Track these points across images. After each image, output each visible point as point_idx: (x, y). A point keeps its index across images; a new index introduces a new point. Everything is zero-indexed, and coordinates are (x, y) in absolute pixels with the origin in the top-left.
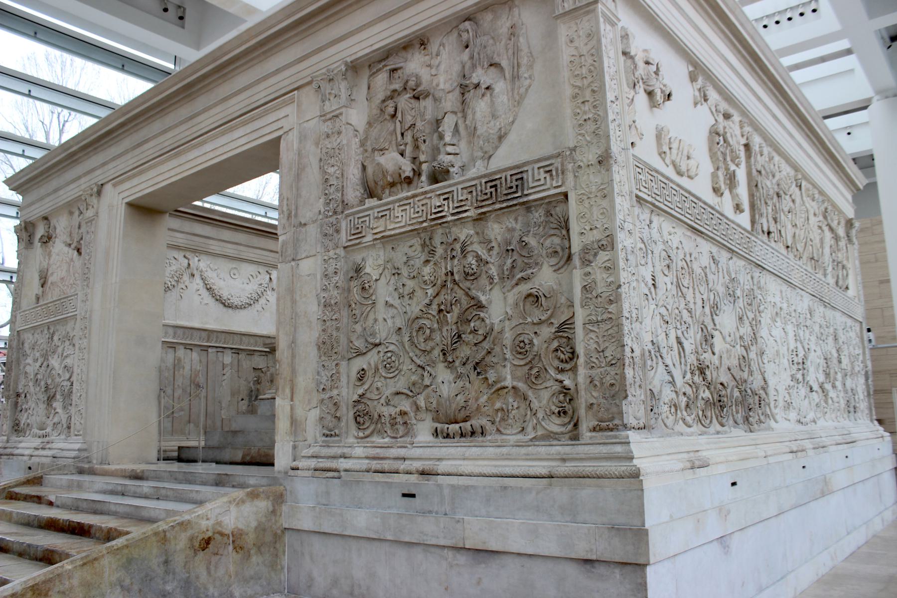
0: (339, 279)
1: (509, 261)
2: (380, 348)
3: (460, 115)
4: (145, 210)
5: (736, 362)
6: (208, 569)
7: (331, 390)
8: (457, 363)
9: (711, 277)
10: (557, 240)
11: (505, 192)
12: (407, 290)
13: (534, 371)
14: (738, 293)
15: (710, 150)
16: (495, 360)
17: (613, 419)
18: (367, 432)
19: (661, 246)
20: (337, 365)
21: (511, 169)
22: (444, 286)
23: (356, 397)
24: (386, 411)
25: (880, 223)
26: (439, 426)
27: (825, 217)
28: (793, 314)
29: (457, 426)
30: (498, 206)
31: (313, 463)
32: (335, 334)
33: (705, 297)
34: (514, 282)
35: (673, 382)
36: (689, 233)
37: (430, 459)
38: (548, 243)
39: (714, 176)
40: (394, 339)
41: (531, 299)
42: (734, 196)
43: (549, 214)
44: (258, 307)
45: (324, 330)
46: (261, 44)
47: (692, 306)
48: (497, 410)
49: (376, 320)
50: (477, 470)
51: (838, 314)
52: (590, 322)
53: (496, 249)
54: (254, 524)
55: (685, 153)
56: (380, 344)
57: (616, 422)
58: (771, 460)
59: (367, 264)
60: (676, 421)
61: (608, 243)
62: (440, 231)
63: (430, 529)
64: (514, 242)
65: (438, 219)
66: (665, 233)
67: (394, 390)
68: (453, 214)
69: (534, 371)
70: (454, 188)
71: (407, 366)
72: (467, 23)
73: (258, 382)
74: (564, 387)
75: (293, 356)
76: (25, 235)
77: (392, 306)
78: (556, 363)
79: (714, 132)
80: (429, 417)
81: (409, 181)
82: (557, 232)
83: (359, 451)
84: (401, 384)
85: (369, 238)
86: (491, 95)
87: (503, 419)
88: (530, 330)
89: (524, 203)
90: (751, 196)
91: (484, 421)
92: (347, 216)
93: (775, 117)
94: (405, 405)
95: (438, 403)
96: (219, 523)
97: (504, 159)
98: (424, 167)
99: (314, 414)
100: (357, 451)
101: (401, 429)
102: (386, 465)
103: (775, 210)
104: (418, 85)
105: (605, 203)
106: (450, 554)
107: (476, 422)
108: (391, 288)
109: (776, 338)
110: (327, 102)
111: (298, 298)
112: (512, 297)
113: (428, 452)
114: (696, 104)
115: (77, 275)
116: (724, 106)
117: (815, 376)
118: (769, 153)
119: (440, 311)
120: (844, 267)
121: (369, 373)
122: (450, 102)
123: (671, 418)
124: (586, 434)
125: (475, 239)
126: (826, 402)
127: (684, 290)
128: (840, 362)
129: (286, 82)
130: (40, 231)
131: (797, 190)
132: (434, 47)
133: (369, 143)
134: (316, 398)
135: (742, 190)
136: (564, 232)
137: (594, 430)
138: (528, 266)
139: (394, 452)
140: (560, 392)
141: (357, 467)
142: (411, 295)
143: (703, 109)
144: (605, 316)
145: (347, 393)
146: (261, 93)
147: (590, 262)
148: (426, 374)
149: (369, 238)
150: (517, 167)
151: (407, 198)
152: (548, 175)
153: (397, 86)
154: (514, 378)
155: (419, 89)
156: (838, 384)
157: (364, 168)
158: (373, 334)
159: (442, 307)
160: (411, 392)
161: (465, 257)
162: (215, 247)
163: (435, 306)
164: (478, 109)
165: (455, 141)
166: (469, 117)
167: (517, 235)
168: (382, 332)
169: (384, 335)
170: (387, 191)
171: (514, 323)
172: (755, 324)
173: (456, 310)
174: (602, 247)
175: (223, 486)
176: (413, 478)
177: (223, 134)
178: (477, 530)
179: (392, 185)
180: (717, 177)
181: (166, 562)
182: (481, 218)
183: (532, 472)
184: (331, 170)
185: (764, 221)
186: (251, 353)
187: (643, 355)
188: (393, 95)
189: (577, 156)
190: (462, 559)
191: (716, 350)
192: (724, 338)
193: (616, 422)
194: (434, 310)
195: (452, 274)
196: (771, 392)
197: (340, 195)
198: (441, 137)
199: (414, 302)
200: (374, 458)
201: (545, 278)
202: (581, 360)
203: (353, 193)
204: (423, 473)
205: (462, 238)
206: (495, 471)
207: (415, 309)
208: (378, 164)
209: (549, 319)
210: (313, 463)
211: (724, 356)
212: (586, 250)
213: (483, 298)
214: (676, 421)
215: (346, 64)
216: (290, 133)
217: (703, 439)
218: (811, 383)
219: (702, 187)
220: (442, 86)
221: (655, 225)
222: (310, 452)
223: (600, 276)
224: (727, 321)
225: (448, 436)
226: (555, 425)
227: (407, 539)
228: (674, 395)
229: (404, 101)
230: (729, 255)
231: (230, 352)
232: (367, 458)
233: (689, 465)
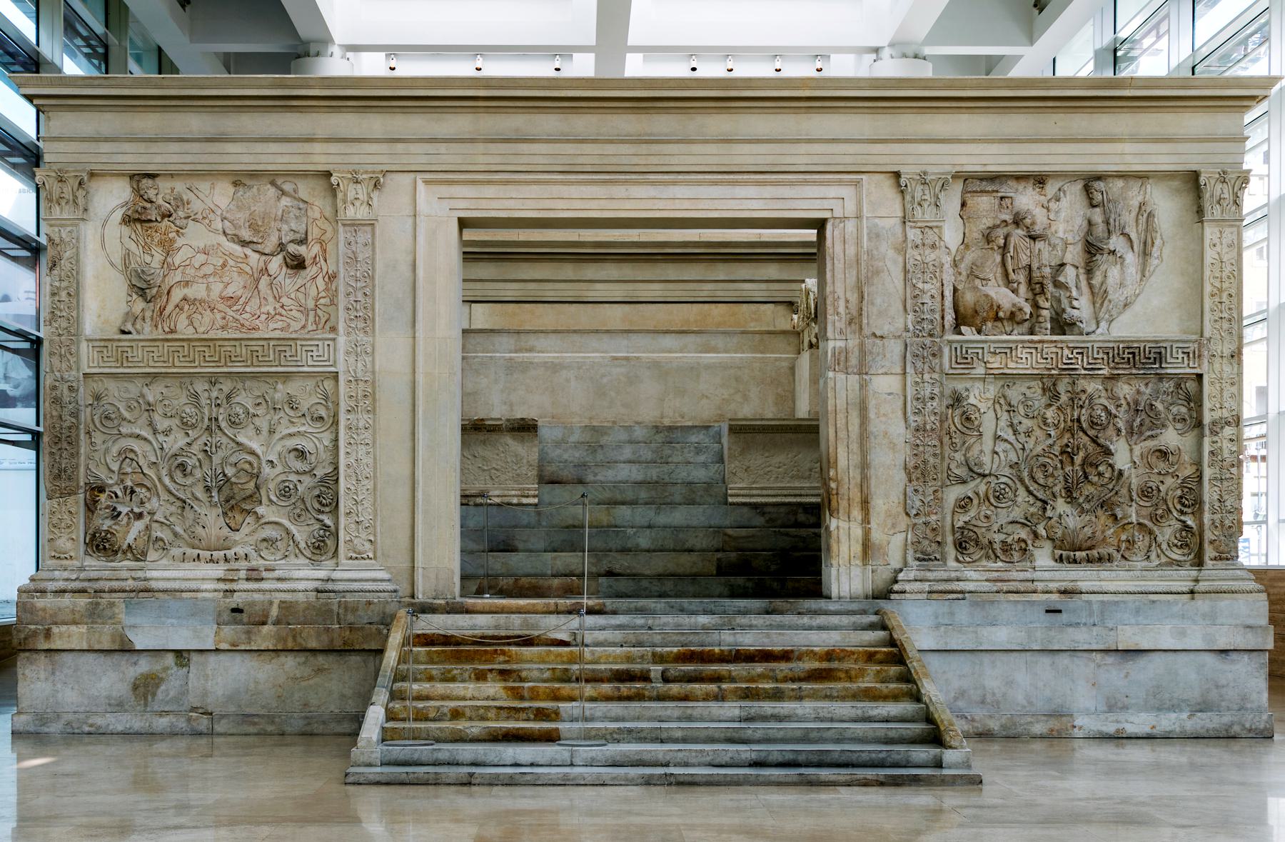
2: (988, 479)
3: (1081, 271)
7: (928, 515)
8: (1081, 500)
10: (1184, 410)
11: (1141, 359)
20: (935, 491)
22: (1070, 430)
24: (998, 538)
29: (1084, 554)
30: (1134, 371)
31: (926, 587)
32: (932, 460)
38: (1175, 409)
40: (1007, 471)
43: (1178, 386)
52: (1215, 479)
53: (1125, 406)
56: (990, 475)
61: (1237, 421)
63: (1082, 638)
65: (1069, 371)
67: (1010, 519)
74: (1187, 526)
75: (865, 478)
78: (1179, 507)
80: (1048, 546)
83: (974, 575)
84: (1017, 514)
85: (980, 370)
86: (1122, 264)
87: (1128, 548)
88: (1156, 478)
91: (1111, 550)
94: (1024, 534)
95: (1064, 534)
98: (1046, 313)
100: (975, 576)
101: (1016, 556)
104: (1033, 223)
105: (1234, 389)
106: (1098, 656)
107: (1104, 551)
108: (1002, 423)
111: (872, 415)
112: (1137, 450)
113: (1057, 575)
115: (284, 300)
119: (1062, 453)
121: (976, 502)
122: (1074, 254)
124: (1209, 563)
125: (1103, 394)
129: (848, 160)
132: (1051, 188)
133: (963, 266)
134: (904, 522)
137: (1215, 559)
139: (1015, 575)
140: (1181, 530)
142: (1028, 434)
145: (947, 518)
146: (800, 156)
149: (980, 370)
150: (1157, 342)
151: (1032, 342)
153: (1008, 218)
157: (955, 290)
158: (980, 465)
160: (1027, 522)
164: (1109, 274)
166: (1097, 281)
170: (989, 324)
171: (1141, 471)
173: (1081, 454)
176: (1055, 597)
177: (715, 183)
178: (1128, 637)
182: (1113, 378)
183: (1174, 590)
184: (920, 285)
189: (1212, 346)
190: (1110, 659)
194: (1057, 450)
195: (1079, 420)
197: (938, 316)
199: (1032, 441)
201: (1171, 437)
202: (1207, 507)
203: (950, 317)
204: (1064, 592)
207: (1037, 444)
208: (987, 296)
210: (926, 587)
212: (1214, 423)
213: (1111, 447)
216: (850, 226)
222: (912, 576)
223: (1226, 445)
225: (1075, 561)
226: (1176, 555)
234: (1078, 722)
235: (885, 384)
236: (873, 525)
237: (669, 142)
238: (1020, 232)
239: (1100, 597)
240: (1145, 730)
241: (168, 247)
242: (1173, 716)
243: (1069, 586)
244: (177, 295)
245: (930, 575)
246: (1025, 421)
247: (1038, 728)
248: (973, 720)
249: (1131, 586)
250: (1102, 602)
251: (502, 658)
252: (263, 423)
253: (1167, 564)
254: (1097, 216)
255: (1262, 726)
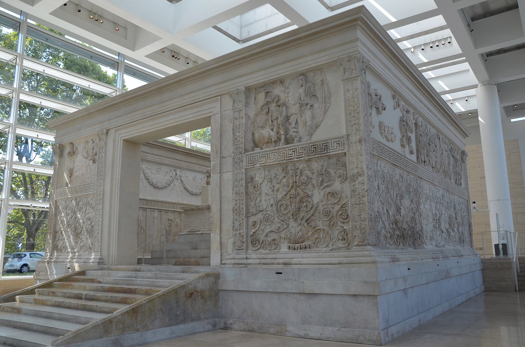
0: (243, 182)
1: (321, 179)
2: (262, 213)
4: (131, 144)
5: (410, 220)
6: (192, 306)
8: (298, 219)
9: (400, 184)
11: (320, 150)
12: (276, 188)
13: (332, 223)
14: (411, 189)
15: (400, 128)
16: (315, 218)
17: (364, 241)
18: (257, 248)
19: (381, 173)
21: (322, 141)
22: (292, 187)
23: (251, 233)
25: (481, 147)
26: (291, 245)
27: (451, 152)
28: (435, 198)
29: (299, 245)
30: (316, 156)
33: (397, 192)
34: (323, 187)
35: (385, 228)
36: (391, 166)
37: (287, 258)
39: (402, 140)
40: (270, 208)
41: (330, 194)
42: (410, 147)
44: (170, 188)
45: (236, 204)
46: (201, 73)
47: (392, 196)
48: (316, 239)
49: (261, 201)
50: (309, 262)
51: (456, 197)
52: (355, 204)
54: (208, 287)
55: (391, 132)
57: (365, 242)
58: (424, 261)
59: (257, 177)
60: (386, 243)
62: (291, 164)
64: (324, 171)
66: (382, 167)
68: (297, 158)
69: (332, 223)
70: (297, 147)
71: (276, 220)
72: (302, 76)
73: (170, 226)
76: (58, 151)
77: (268, 195)
78: (341, 219)
79: (402, 120)
80: (286, 241)
81: (275, 142)
82: (341, 168)
83: (254, 256)
84: (274, 227)
85: (258, 165)
89: (327, 156)
90: (417, 146)
92: (248, 155)
93: (428, 108)
95: (290, 235)
96: (195, 287)
97: (319, 136)
99: (231, 241)
101: (274, 247)
102: (268, 261)
103: (428, 151)
104: (279, 100)
107: (306, 243)
109: (427, 208)
110: (235, 104)
112: (322, 194)
113: (286, 255)
114: (395, 109)
116: (407, 107)
117: (444, 226)
118: (425, 125)
120: (459, 174)
123: (385, 242)
125: (307, 168)
126: (449, 237)
127: (390, 190)
128: (456, 219)
130: (68, 150)
131: (438, 141)
132: (287, 84)
135: (413, 144)
136: (344, 168)
138: (329, 181)
139: (271, 256)
141: (254, 262)
143: (398, 110)
144: (362, 202)
147: (355, 181)
148: (285, 223)
149: (258, 165)
151: (276, 150)
152: (338, 145)
154: (323, 226)
155: (280, 102)
156: (455, 229)
157: (253, 134)
159: (292, 196)
161: (302, 175)
162: (150, 157)
163: (288, 196)
165: (296, 127)
167: (324, 168)
168: (264, 205)
169: (265, 207)
170: (265, 145)
172: (418, 203)
174: (361, 175)
175: (186, 272)
176: (281, 266)
177: (180, 112)
178: (309, 286)
179: (267, 143)
180: (403, 140)
181: (177, 302)
182: (309, 160)
184: (238, 134)
185: (422, 156)
186: (167, 211)
187: (375, 217)
188: (268, 103)
189: (350, 138)
190: (303, 298)
191: (402, 214)
192: (405, 209)
193: (365, 242)
195: (296, 182)
196: (425, 232)
198: (290, 124)
200: (262, 259)
201: (337, 186)
204: (285, 264)
205: (301, 168)
206: (317, 262)
208: (261, 133)
209: (338, 202)
210: (233, 261)
211: (405, 217)
212: (353, 175)
213: (310, 193)
214: (386, 243)
215: (246, 88)
217: (397, 251)
218: (442, 228)
219: (396, 146)
220: (290, 102)
221: (379, 164)
222: (231, 257)
224: (406, 202)
225: (295, 249)
226: (340, 244)
227: (279, 291)
228: (385, 233)
229: (273, 107)
230: (407, 174)
231: (156, 211)
232: (258, 259)
233: (392, 260)
234: (289, 329)
235: (228, 176)
236: (222, 235)
237: (167, 101)
238: (274, 104)
239: (299, 266)
240: (318, 335)
241: (74, 162)
242: (331, 328)
243: (287, 261)
244: (74, 175)
245: (237, 256)
246: (276, 185)
247: (272, 330)
248: (247, 324)
249: (314, 261)
250: (299, 269)
251: (71, 287)
252: (84, 210)
253: (335, 249)
254: (301, 90)
255: (375, 339)
